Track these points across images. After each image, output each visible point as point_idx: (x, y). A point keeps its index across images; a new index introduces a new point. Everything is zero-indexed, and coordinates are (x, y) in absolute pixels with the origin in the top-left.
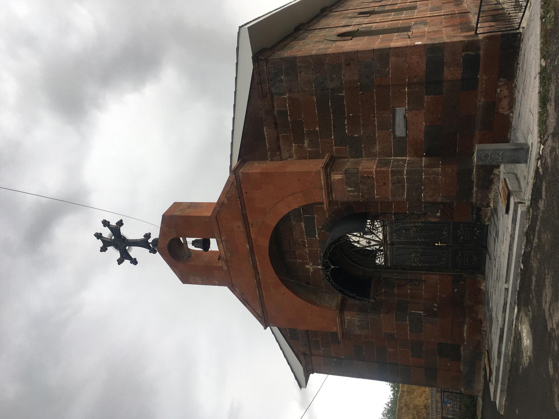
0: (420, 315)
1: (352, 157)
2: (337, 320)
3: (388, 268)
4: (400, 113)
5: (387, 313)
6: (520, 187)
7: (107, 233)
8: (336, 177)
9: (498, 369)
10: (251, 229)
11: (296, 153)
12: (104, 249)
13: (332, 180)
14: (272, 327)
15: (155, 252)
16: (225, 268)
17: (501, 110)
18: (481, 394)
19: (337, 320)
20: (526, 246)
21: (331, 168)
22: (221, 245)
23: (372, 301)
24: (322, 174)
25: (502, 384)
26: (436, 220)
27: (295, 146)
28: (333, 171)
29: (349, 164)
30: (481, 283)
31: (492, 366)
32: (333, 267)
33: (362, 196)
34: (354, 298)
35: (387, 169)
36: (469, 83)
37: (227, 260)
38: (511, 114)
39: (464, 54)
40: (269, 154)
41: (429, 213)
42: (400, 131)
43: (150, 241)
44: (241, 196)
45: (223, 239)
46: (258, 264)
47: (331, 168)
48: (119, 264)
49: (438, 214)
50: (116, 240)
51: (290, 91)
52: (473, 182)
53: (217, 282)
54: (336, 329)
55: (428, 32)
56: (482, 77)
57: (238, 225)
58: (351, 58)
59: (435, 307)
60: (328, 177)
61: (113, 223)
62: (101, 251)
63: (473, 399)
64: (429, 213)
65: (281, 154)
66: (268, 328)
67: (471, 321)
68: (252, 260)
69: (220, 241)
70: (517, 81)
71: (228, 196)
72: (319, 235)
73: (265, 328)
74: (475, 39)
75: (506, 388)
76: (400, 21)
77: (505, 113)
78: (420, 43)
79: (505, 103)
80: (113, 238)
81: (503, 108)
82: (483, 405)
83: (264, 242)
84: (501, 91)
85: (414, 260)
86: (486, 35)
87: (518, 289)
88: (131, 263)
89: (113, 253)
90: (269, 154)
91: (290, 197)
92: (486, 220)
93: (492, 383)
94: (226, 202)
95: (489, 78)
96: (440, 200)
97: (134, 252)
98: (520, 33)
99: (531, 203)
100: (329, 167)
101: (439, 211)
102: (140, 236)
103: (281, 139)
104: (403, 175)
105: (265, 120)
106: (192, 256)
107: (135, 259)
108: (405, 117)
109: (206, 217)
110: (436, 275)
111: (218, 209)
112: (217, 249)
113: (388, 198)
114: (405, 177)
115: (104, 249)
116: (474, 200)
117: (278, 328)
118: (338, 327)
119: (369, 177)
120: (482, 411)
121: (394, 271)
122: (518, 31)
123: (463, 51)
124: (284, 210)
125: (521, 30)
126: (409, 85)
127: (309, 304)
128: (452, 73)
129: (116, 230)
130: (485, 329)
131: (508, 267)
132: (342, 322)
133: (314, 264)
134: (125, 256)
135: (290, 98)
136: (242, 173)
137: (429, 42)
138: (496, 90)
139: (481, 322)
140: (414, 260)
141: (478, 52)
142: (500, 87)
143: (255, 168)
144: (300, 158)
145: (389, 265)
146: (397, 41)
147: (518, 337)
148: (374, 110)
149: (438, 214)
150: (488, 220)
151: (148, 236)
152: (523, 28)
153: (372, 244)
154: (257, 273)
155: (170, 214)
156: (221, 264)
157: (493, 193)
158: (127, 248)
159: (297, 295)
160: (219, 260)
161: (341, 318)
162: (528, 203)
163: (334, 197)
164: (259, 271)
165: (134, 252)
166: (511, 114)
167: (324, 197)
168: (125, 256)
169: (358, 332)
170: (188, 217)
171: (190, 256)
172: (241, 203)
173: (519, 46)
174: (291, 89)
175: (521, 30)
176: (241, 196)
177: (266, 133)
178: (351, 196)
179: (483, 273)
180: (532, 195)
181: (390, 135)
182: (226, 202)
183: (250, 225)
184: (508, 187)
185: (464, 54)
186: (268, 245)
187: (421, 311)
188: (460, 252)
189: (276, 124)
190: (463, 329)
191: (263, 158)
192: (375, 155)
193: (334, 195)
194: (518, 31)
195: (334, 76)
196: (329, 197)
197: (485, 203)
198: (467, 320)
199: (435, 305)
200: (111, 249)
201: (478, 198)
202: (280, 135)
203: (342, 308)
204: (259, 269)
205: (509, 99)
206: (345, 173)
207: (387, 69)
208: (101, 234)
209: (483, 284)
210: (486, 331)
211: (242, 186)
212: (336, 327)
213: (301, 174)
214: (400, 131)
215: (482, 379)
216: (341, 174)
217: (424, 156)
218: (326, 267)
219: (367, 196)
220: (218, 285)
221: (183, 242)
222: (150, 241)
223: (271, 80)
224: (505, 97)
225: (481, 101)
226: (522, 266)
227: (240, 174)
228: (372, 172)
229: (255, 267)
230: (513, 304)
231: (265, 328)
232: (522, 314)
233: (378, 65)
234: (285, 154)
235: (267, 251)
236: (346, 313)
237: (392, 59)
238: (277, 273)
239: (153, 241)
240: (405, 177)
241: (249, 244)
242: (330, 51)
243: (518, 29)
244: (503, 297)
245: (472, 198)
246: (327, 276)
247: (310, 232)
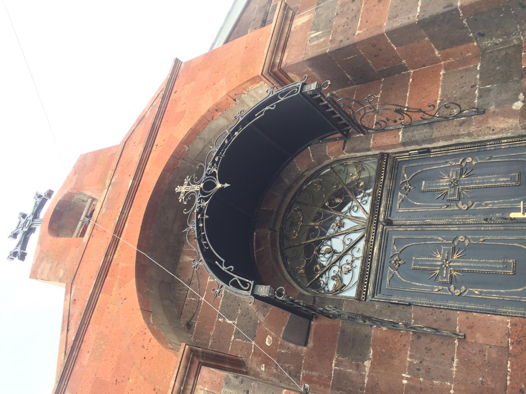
13: (292, 29)
32: (219, 185)
33: (331, 41)
34: (225, 278)
53: (61, 273)
64: (492, 108)
68: (122, 213)
85: (441, 270)
101: (521, 96)
127: (149, 334)
140: (441, 270)
149: (518, 105)
153: (346, 227)
159: (146, 311)
172: (160, 107)
183: (154, 147)
193: (286, 54)
216: (310, 13)
219: (341, 37)
241: (134, 179)
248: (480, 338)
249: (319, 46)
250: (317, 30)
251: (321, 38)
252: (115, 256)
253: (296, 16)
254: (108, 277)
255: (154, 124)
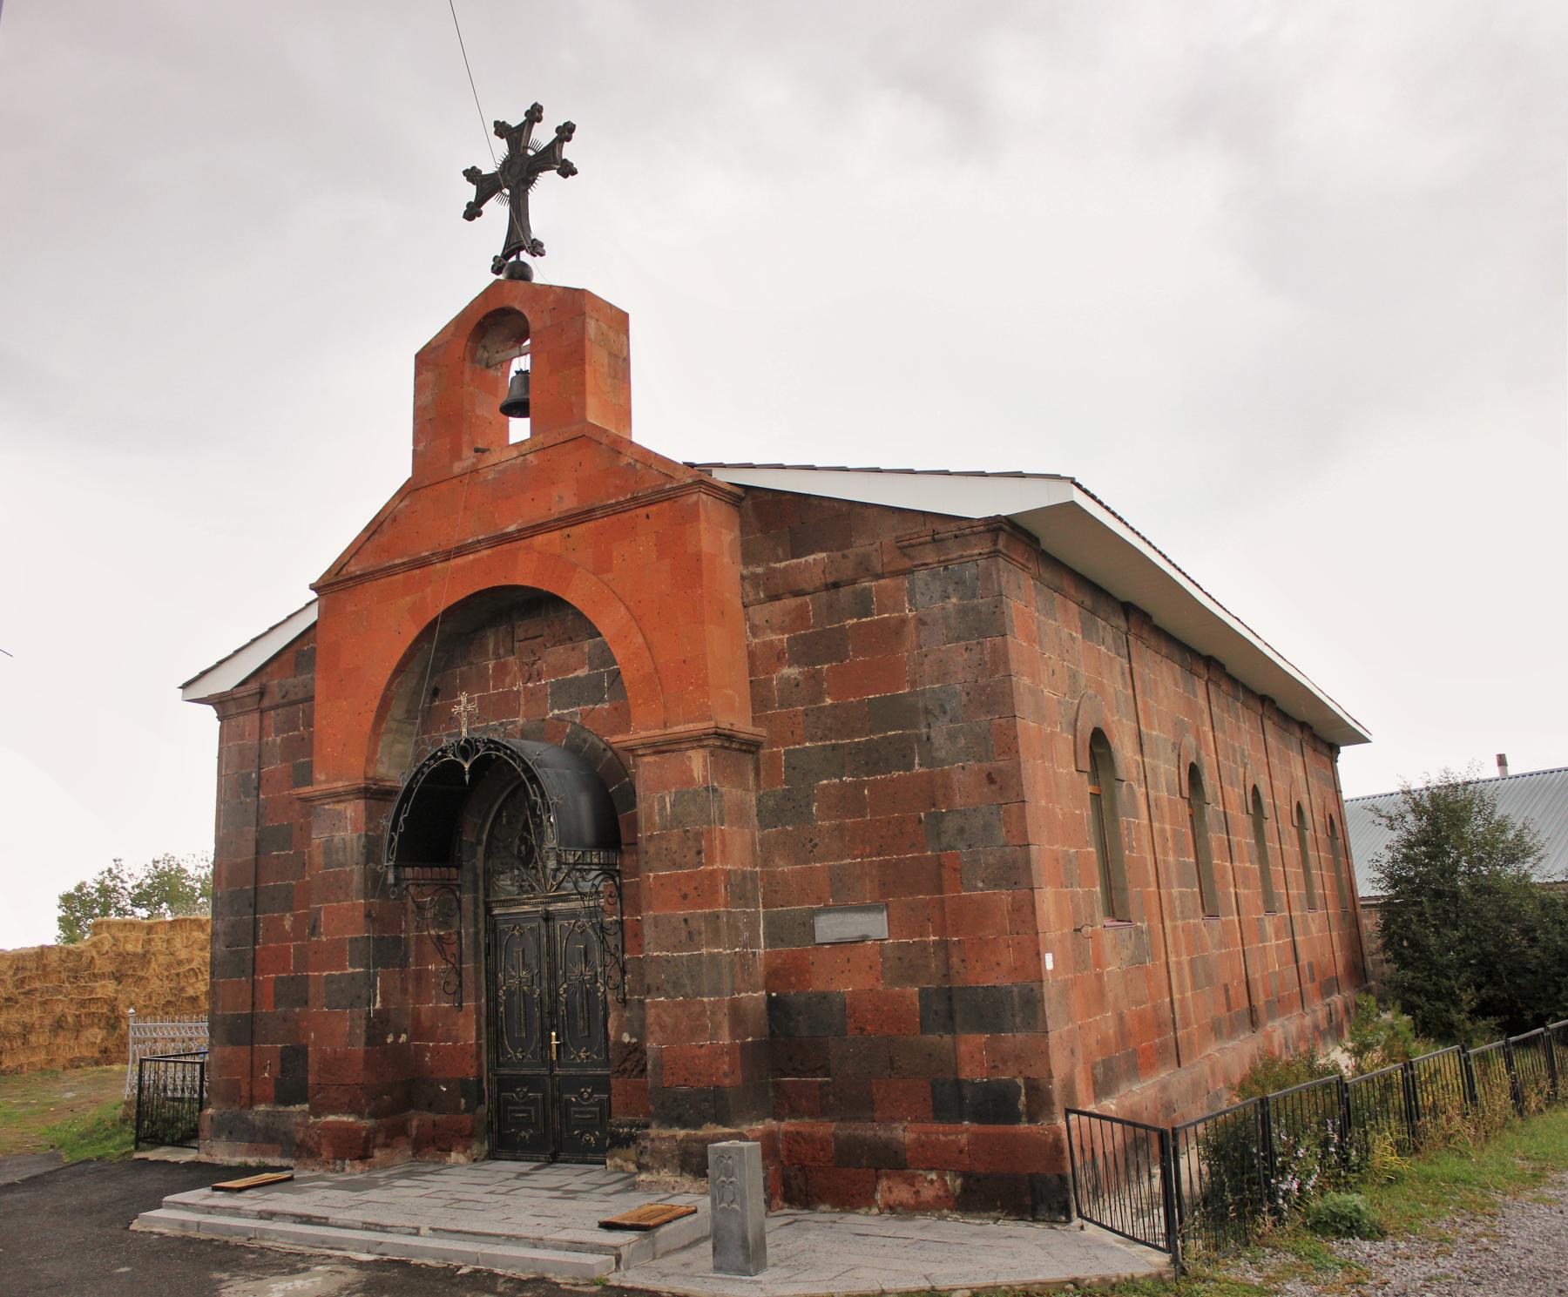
0: (370, 1001)
1: (759, 800)
2: (340, 784)
3: (488, 910)
4: (874, 925)
5: (368, 915)
6: (667, 1253)
7: (542, 135)
8: (697, 763)
9: (236, 1212)
10: (557, 534)
11: (765, 644)
12: (501, 129)
13: (690, 753)
14: (316, 606)
15: (497, 270)
16: (457, 468)
17: (884, 1184)
18: (203, 1158)
19: (340, 784)
20: (511, 1279)
21: (722, 746)
22: (515, 454)
23: (391, 878)
24: (700, 726)
25: (199, 1224)
26: (612, 1033)
27: (781, 641)
28: (712, 754)
29: (742, 794)
30: (464, 1152)
31: (248, 1193)
32: (467, 766)
34: (394, 828)
35: (722, 900)
36: (951, 1099)
37: (477, 471)
38: (875, 1210)
39: (1020, 1081)
40: (760, 570)
41: (627, 1014)
42: (830, 927)
43: (525, 256)
44: (638, 502)
45: (530, 457)
46: (471, 557)
47: (722, 746)
48: (466, 173)
49: (626, 1038)
50: (524, 163)
51: (921, 622)
52: (698, 1126)
54: (322, 782)
55: (1099, 977)
56: (964, 1132)
57: (564, 500)
58: (1004, 784)
59: (397, 1037)
60: (697, 741)
61: (568, 152)
62: (496, 123)
63: (188, 1138)
64: (627, 1014)
65: (760, 602)
66: (314, 595)
67: (364, 1134)
69: (524, 449)
70: (956, 1220)
71: (638, 466)
72: (559, 718)
73: (313, 587)
74: (1058, 1109)
75: (191, 1234)
76: (1153, 888)
77: (878, 1196)
78: (1049, 965)
79: (903, 1193)
80: (531, 153)
81: (890, 1189)
82: (177, 1163)
83: (524, 573)
84: (932, 1182)
86: (1065, 1135)
87: (414, 1261)
88: (469, 204)
89: (492, 155)
90: (760, 570)
91: (640, 640)
92: (618, 1161)
93: (208, 1197)
94: (625, 461)
95: (961, 1151)
96: (651, 1045)
97: (497, 211)
98: (1069, 1220)
99: (613, 1287)
100: (726, 743)
102: (537, 229)
103: (799, 600)
104: (708, 944)
105: (844, 557)
106: (492, 372)
107: (479, 214)
108: (864, 939)
109: (583, 408)
110: (478, 1037)
111: (604, 440)
112: (512, 441)
113: (649, 908)
114: (704, 951)
115: (501, 129)
116: (653, 1131)
117: (314, 625)
118: (324, 787)
119: (699, 853)
120: (165, 1162)
121: (482, 925)
122: (1074, 1214)
123: (1027, 1079)
124: (610, 621)
125: (1077, 1221)
126: (943, 945)
127: (376, 703)
128: (973, 1057)
129: (552, 159)
130: (348, 1169)
131: (474, 1234)
132: (337, 797)
133: (470, 715)
134: (486, 186)
135: (904, 621)
136: (696, 504)
137: (1050, 990)
138: (932, 1169)
139: (364, 1157)
141: (1024, 1118)
142: (942, 1178)
143: (718, 538)
144: (751, 655)
145: (496, 912)
146: (1060, 902)
147: (301, 1265)
148: (879, 855)
150: (616, 1166)
151: (537, 249)
152: (1082, 1228)
154: (447, 556)
155: (588, 310)
156: (468, 459)
157: (672, 1179)
158: (507, 191)
160: (477, 450)
161: (347, 793)
162: (614, 1280)
163: (645, 759)
164: (453, 562)
165: (497, 211)
166: (875, 1210)
167: (643, 734)
168: (486, 186)
169: (318, 837)
170: (583, 361)
171: (488, 366)
172: (618, 503)
173: (1038, 1221)
174: (924, 623)
175: (1077, 1221)
176: (638, 502)
177: (811, 558)
178: (651, 807)
179: (492, 1156)
180: (632, 1290)
181: (819, 900)
182: (625, 461)
183: (566, 531)
184: (669, 1222)
185: (1020, 1081)
186: (518, 582)
187: (383, 1000)
188: (539, 1095)
189: (836, 585)
190: (344, 1113)
191: (748, 555)
192: (765, 863)
194: (1074, 1214)
195: (962, 742)
196: (645, 746)
197: (645, 1159)
198: (368, 1123)
199: (403, 1038)
200: (501, 148)
201: (657, 1143)
202: (808, 598)
203: (374, 794)
204: (459, 561)
205: (912, 1202)
206: (707, 789)
207: (980, 885)
208: (539, 120)
209: (462, 1159)
210: (343, 1170)
211: (666, 504)
212: (326, 781)
213: (691, 675)
214: (830, 927)
215: (237, 1160)
216: (705, 778)
217: (769, 995)
218: (466, 749)
219: (652, 850)
220: (414, 451)
221: (523, 346)
222: (525, 256)
223: (946, 568)
224: (918, 1192)
225: (904, 1133)
226: (464, 1271)
227: (694, 497)
228: (711, 861)
229: (461, 551)
230: (380, 1249)
231: (313, 587)
232: (352, 1275)
233: (991, 860)
234: (760, 614)
235: (503, 582)
236: (361, 803)
237: (1005, 897)
238: (449, 612)
239: (525, 265)
240: (704, 951)
241: (519, 531)
242: (1027, 725)
243: (1080, 1215)
244: (398, 1223)
245: (659, 1126)
246: (444, 751)
247: (568, 692)
248: (461, 1021)
249: (650, 818)
250: (673, 805)
251: (661, 815)
252: (439, 566)
253: (706, 752)
254: (418, 572)
255: (593, 510)
